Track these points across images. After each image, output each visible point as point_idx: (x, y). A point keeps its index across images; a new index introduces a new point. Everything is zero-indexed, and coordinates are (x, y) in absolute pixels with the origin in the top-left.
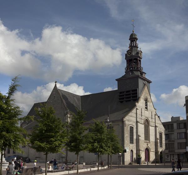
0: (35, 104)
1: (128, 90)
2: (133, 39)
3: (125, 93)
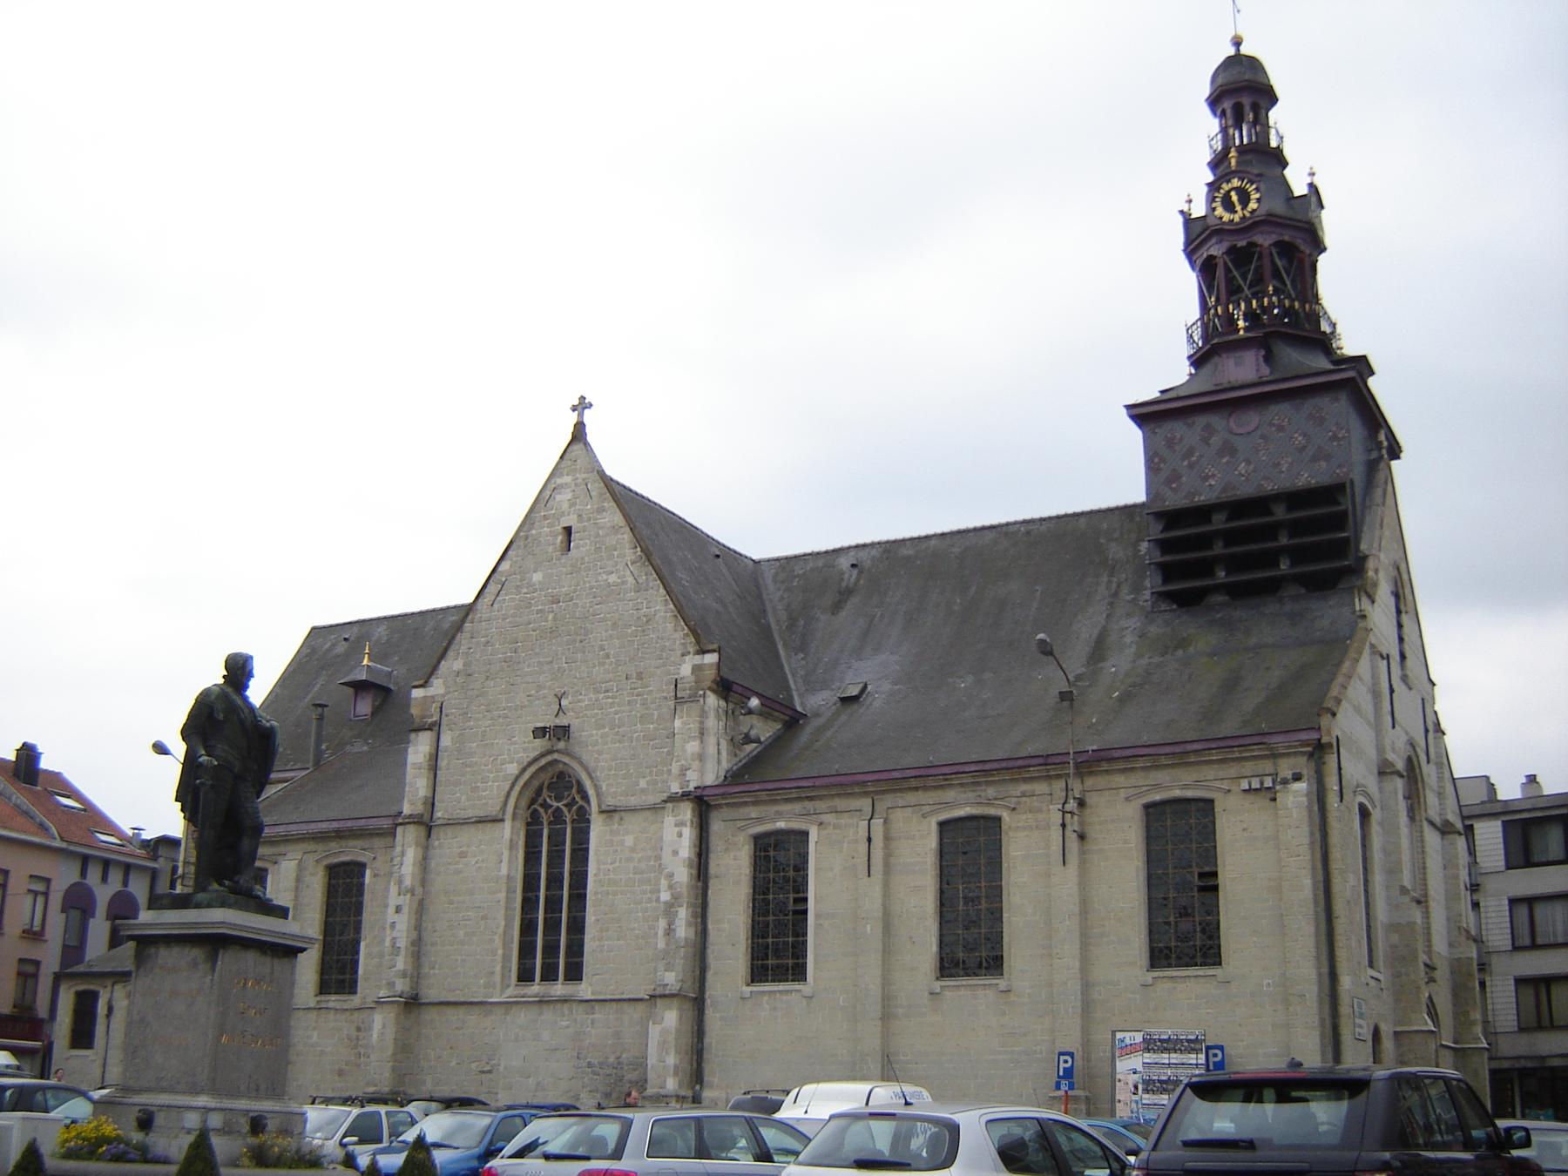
0: (316, 632)
1: (1246, 490)
2: (1242, 92)
3: (1219, 521)
